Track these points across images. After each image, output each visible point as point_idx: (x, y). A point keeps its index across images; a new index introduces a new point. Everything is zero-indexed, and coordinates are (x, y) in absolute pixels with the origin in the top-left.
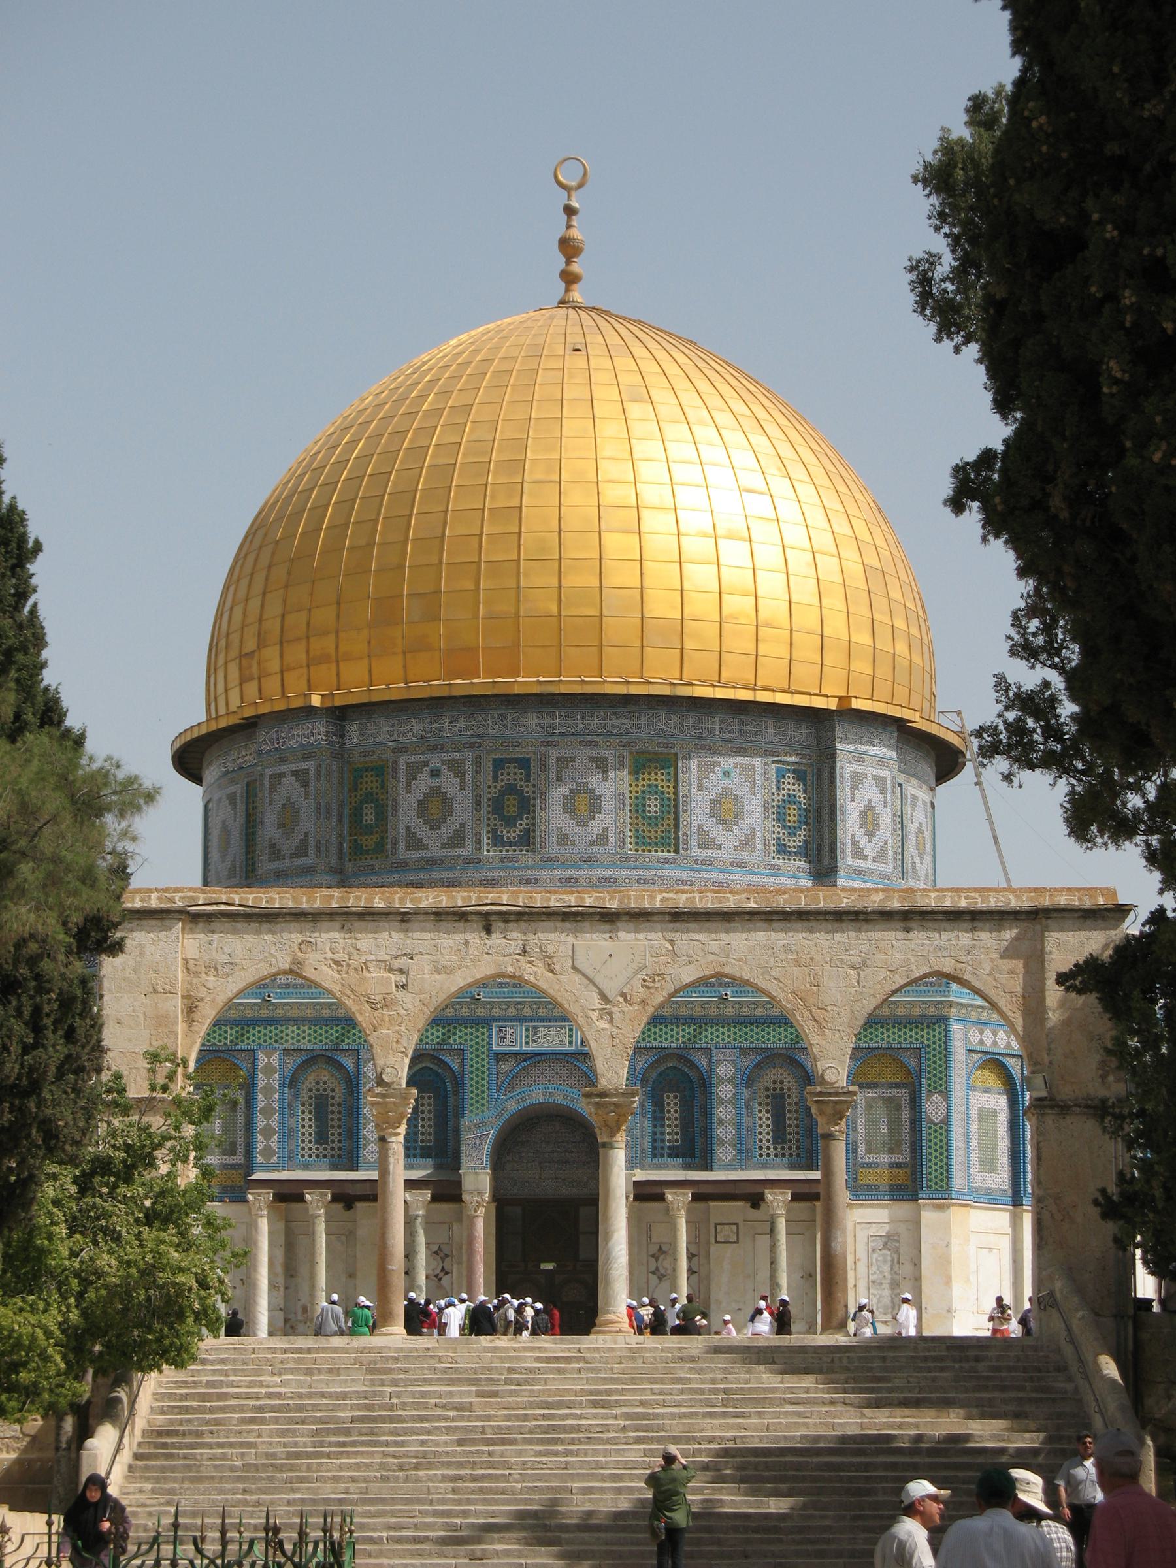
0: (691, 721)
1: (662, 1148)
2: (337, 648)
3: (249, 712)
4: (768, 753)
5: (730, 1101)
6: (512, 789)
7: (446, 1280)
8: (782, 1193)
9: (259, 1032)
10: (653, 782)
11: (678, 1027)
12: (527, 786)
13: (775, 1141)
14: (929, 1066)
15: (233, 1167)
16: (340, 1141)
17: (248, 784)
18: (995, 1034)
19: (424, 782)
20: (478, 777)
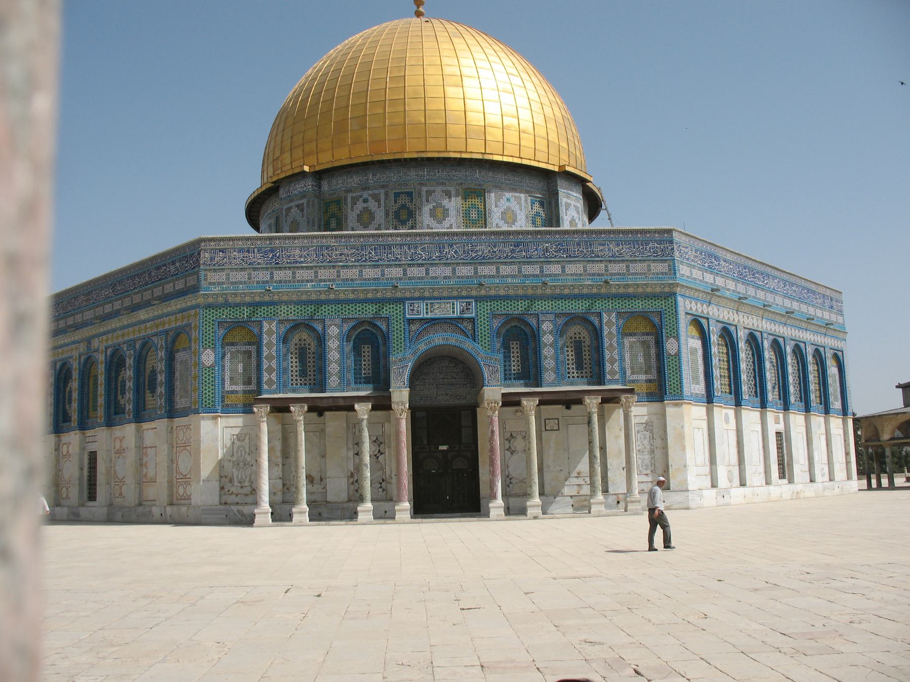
0: (491, 174)
1: (510, 374)
2: (317, 146)
3: (274, 179)
4: (527, 192)
5: (551, 345)
6: (404, 207)
7: (381, 458)
8: (595, 398)
9: (264, 310)
11: (518, 301)
12: (412, 205)
13: (577, 368)
14: (667, 322)
15: (250, 392)
16: (314, 375)
17: (277, 218)
18: (696, 305)
19: (360, 205)
20: (387, 201)
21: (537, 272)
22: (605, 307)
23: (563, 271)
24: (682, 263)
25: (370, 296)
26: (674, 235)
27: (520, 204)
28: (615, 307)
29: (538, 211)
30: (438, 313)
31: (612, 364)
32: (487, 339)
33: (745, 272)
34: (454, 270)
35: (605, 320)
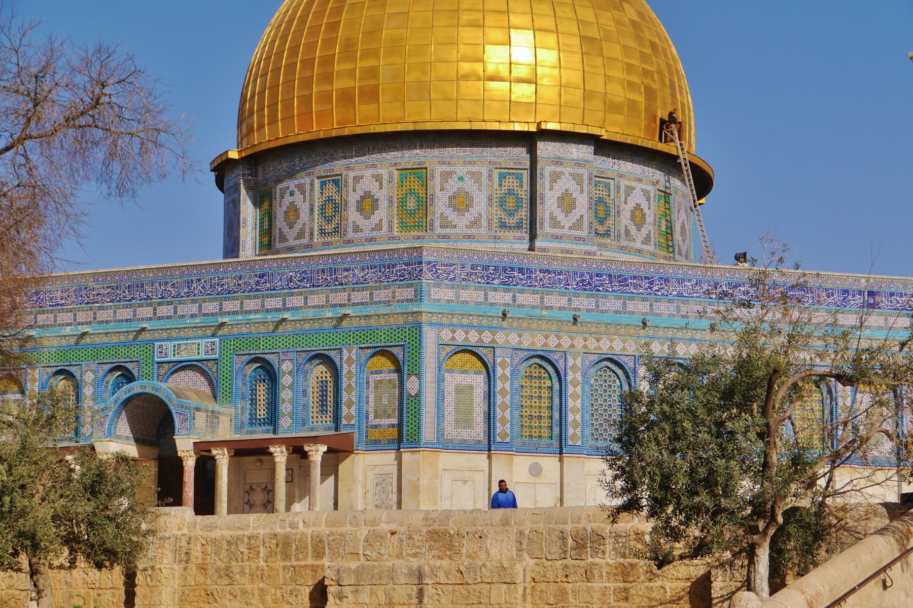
5: (290, 387)
6: (330, 199)
10: (412, 187)
14: (409, 357)
19: (288, 199)
21: (280, 305)
22: (347, 342)
23: (306, 303)
24: (438, 286)
25: (122, 338)
26: (425, 253)
27: (480, 184)
28: (356, 342)
29: (511, 188)
30: (184, 357)
31: (349, 407)
32: (229, 382)
33: (597, 281)
34: (200, 306)
35: (345, 358)
